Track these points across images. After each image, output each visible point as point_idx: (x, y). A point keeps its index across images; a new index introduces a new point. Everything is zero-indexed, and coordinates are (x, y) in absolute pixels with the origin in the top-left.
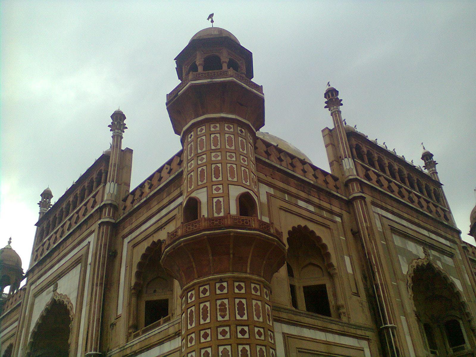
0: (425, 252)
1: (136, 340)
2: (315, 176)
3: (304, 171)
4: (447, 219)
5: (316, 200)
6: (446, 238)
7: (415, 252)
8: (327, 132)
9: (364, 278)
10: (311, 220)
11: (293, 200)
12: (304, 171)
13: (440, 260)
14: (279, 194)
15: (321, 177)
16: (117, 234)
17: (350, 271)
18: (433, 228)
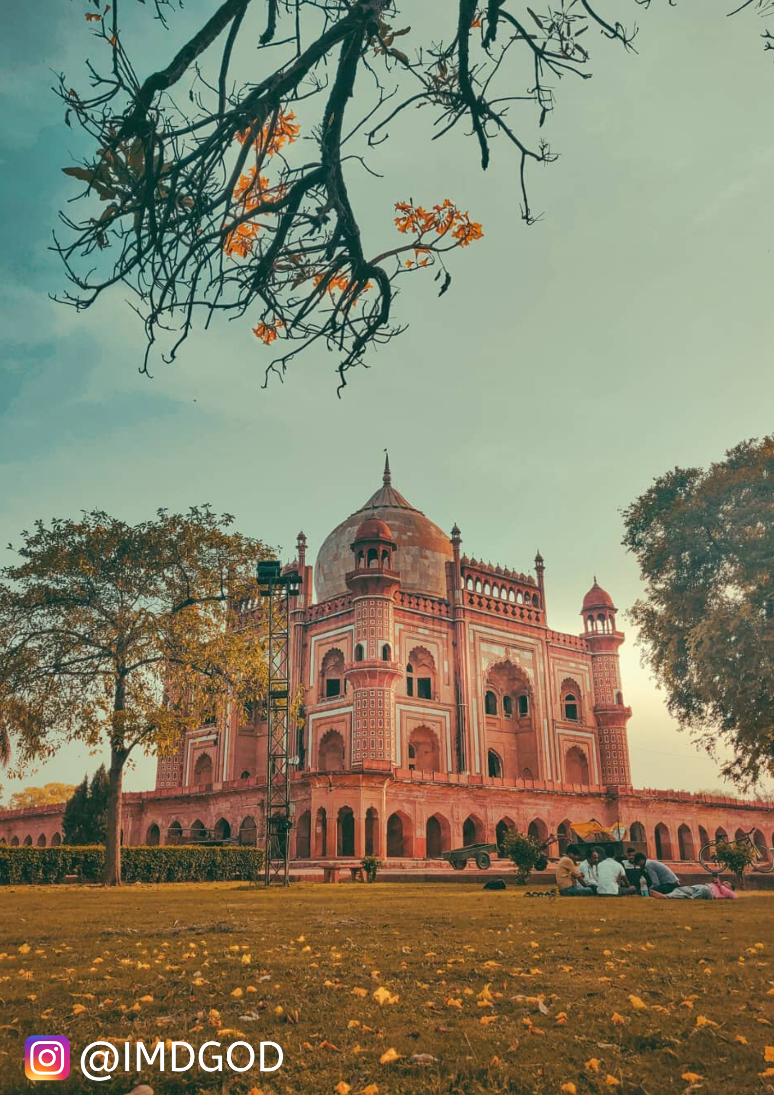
0: (507, 652)
1: (324, 704)
2: (433, 608)
3: (425, 606)
4: (537, 619)
5: (431, 626)
6: (531, 637)
7: (497, 653)
8: (448, 565)
9: (455, 673)
10: (426, 641)
11: (415, 629)
12: (425, 606)
13: (518, 655)
14: (407, 627)
15: (437, 606)
16: (306, 631)
17: (446, 670)
18: (520, 631)
